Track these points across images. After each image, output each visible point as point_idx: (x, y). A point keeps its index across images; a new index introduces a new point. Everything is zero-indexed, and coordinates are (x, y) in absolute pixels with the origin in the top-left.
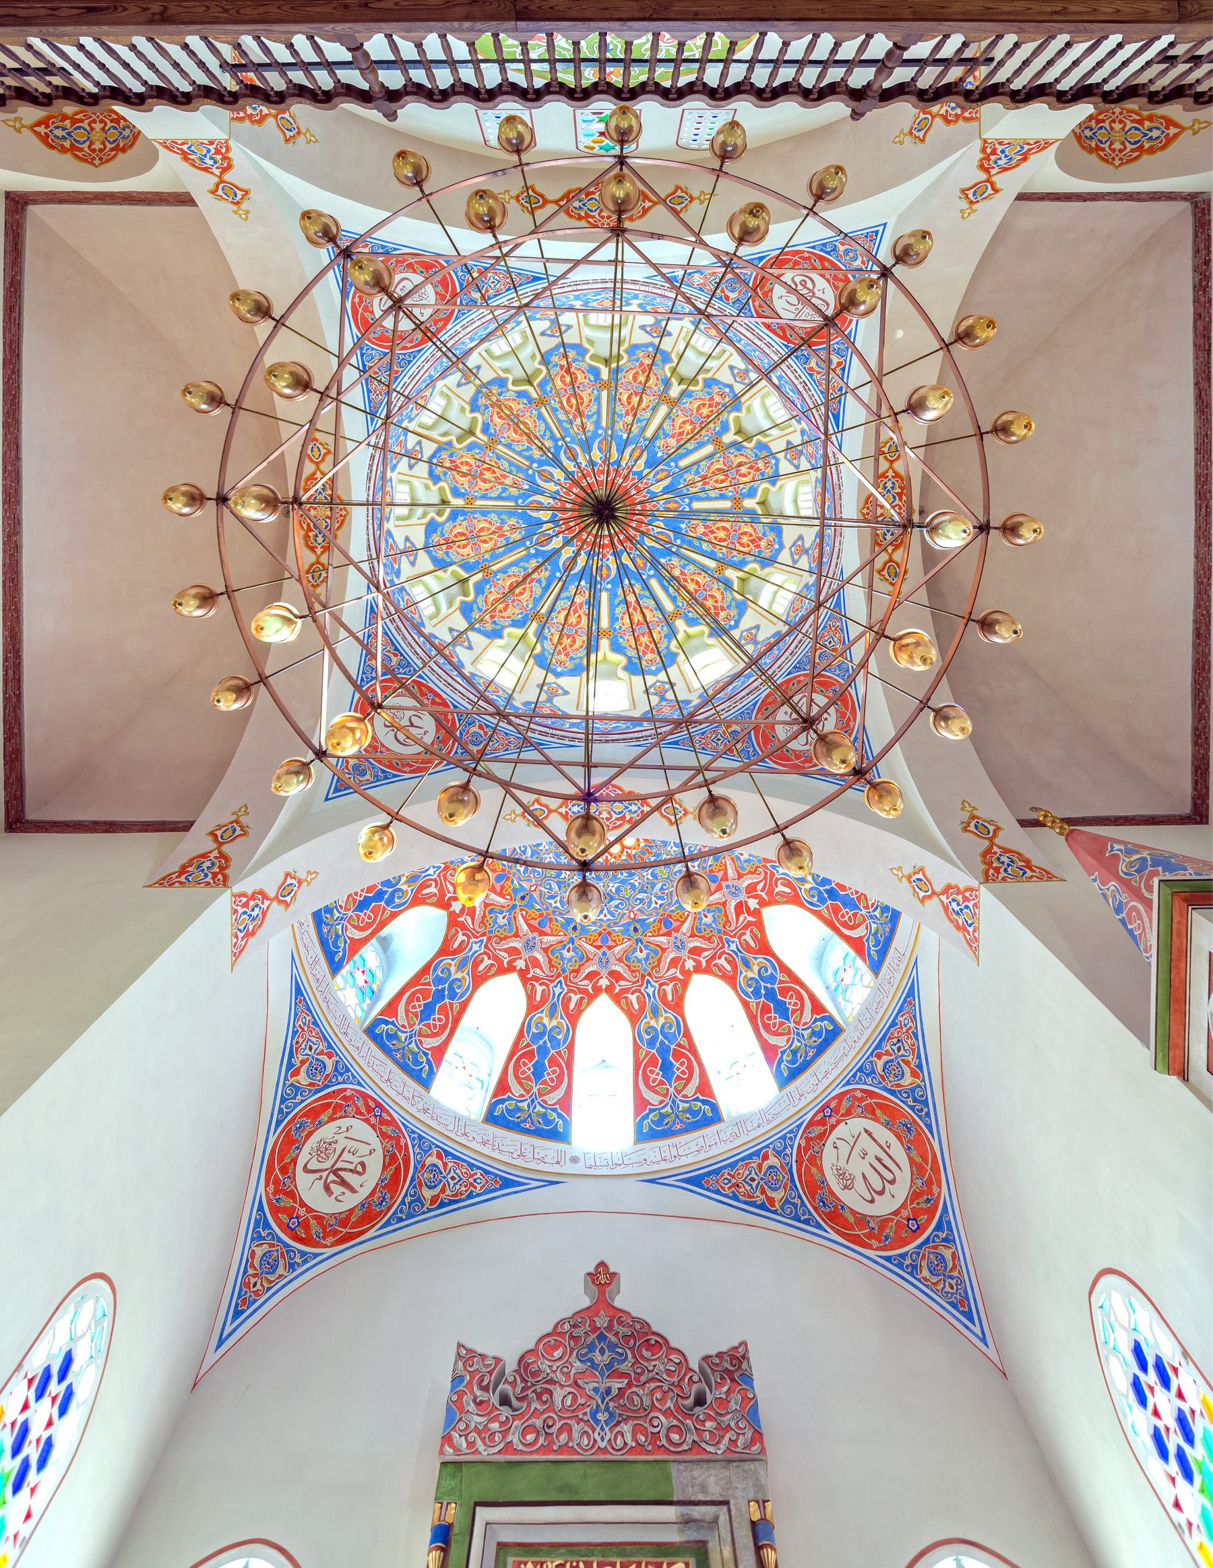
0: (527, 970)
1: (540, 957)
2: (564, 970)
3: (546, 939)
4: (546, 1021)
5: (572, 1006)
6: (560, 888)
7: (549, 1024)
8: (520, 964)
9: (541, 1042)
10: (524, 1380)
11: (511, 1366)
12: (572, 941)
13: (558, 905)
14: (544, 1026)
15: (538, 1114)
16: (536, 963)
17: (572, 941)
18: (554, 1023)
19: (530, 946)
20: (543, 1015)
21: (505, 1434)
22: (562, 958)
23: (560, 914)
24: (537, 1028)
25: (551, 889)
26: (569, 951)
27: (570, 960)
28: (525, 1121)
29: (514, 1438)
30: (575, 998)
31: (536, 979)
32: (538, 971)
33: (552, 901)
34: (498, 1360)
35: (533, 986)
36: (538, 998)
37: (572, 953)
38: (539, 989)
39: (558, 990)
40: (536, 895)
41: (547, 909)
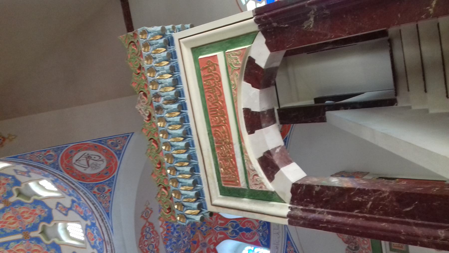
0: (214, 243)
1: (208, 239)
2: (211, 228)
3: (200, 239)
4: (230, 231)
5: (223, 222)
6: (180, 240)
7: (231, 229)
8: (212, 247)
9: (238, 231)
10: (351, 243)
11: (347, 245)
12: (199, 228)
13: (186, 238)
14: (233, 231)
15: (262, 228)
16: (210, 240)
17: (199, 228)
18: (230, 227)
19: (204, 245)
20: (228, 232)
21: (366, 249)
22: (206, 230)
23: (190, 236)
24: (233, 234)
25: (181, 244)
26: (203, 228)
27: (206, 227)
28: (266, 233)
29: (366, 247)
30: (220, 222)
31: (216, 239)
32: (213, 238)
33: (186, 242)
34: (347, 250)
35: (219, 239)
36: (222, 236)
37: (204, 227)
38: (220, 236)
39: (218, 229)
40: (185, 249)
41: (189, 242)
